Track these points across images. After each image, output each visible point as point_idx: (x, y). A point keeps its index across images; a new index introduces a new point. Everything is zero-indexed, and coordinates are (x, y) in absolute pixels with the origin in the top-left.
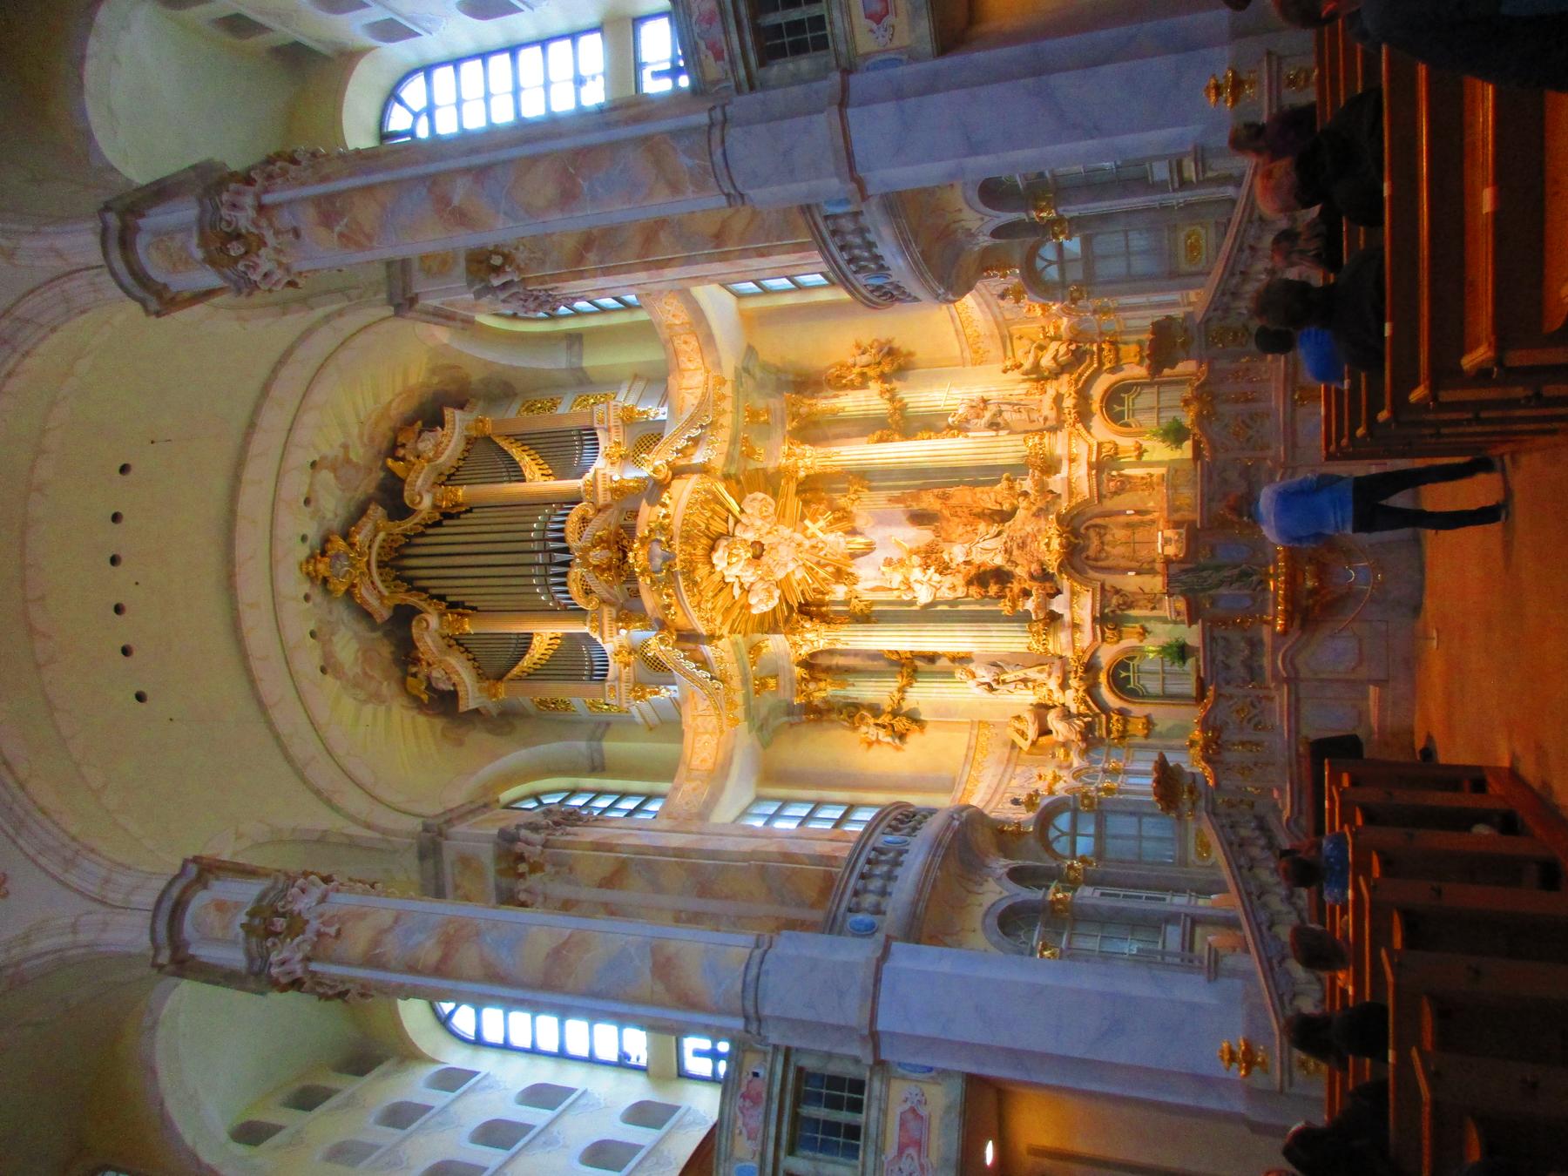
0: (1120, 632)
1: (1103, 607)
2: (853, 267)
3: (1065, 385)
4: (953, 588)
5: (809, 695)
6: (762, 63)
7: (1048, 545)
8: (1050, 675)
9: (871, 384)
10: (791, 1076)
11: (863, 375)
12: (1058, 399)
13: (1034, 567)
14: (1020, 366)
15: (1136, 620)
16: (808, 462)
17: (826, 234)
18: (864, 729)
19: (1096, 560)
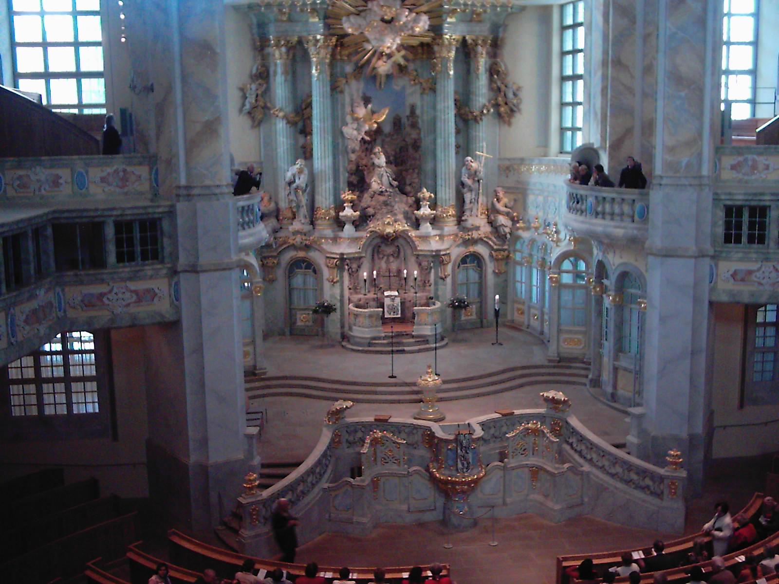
0: (334, 268)
1: (350, 259)
2: (600, 199)
3: (485, 229)
4: (353, 152)
5: (277, 45)
6: (725, 206)
7: (389, 224)
8: (303, 224)
9: (492, 94)
10: (156, 216)
11: (499, 89)
12: (477, 228)
13: (371, 211)
14: (499, 202)
15: (342, 277)
16: (445, 54)
17: (625, 197)
18: (254, 87)
19: (378, 252)
